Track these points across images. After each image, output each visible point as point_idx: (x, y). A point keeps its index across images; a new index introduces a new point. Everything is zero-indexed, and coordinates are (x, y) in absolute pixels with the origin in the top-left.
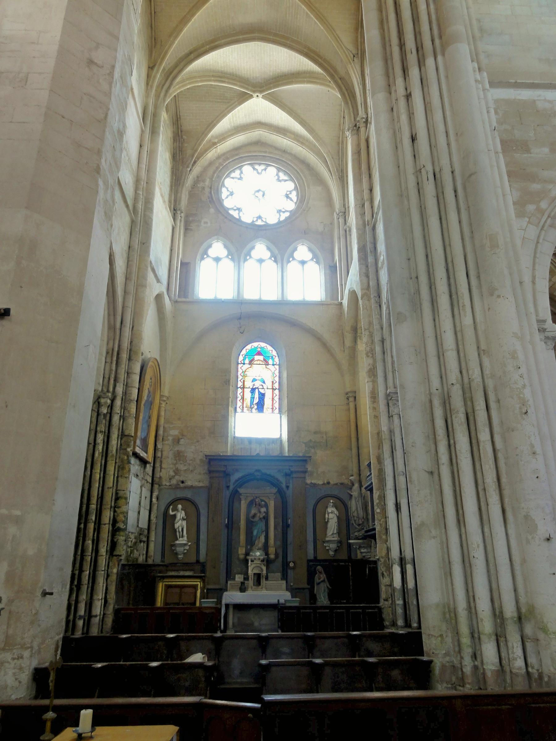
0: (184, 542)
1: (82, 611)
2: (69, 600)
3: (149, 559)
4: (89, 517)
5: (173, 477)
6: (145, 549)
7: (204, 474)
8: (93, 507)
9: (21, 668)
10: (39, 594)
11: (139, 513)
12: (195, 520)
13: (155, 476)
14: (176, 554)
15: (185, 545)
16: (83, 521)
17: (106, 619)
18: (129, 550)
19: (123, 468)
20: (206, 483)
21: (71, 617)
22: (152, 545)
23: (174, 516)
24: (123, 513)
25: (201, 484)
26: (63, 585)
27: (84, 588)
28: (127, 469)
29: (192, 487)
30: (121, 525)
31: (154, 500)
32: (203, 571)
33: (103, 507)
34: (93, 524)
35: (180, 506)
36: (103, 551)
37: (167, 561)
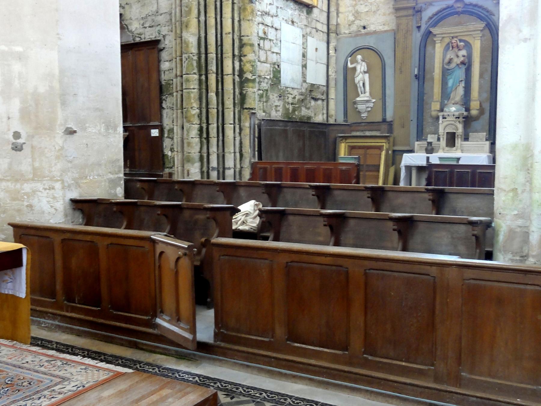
0: (367, 99)
1: (214, 163)
2: (200, 152)
3: (329, 119)
4: (209, 68)
5: (353, 22)
6: (325, 108)
7: (389, 14)
8: (212, 56)
9: (54, 198)
10: (60, 131)
11: (304, 66)
12: (379, 73)
13: (331, 23)
14: (359, 112)
15: (367, 101)
16: (203, 72)
17: (243, 173)
18: (291, 107)
19: (245, 9)
20: (392, 26)
21: (205, 169)
22: (332, 104)
23: (355, 69)
24: (250, 62)
25: (386, 28)
26: (109, 126)
27: (214, 141)
28: (249, 10)
29: (375, 32)
30: (249, 76)
31: (332, 52)
32: (390, 129)
33: (224, 56)
34: (214, 75)
35: (359, 57)
36: (229, 103)
37: (351, 121)
